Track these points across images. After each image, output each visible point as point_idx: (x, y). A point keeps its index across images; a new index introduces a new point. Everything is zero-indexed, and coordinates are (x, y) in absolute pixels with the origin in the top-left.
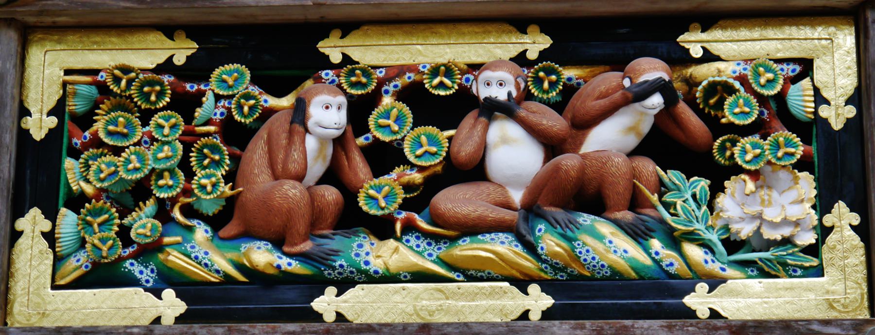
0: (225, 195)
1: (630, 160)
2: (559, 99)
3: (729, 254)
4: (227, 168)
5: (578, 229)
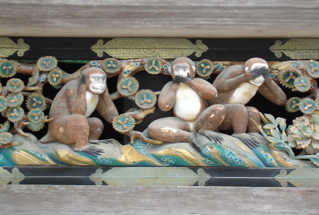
0: (44, 122)
1: (247, 109)
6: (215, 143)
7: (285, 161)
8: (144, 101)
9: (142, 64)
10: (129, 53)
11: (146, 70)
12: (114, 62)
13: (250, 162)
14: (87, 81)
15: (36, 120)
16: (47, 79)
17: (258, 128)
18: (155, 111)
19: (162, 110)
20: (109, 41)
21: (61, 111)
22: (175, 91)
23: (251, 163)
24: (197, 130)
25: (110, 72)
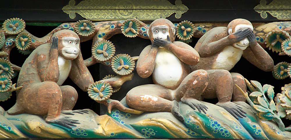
0: (12, 90)
1: (231, 75)
2: (191, 41)
4: (13, 76)
5: (207, 110)
6: (199, 112)
8: (121, 67)
10: (104, 15)
11: (123, 32)
13: (237, 134)
14: (59, 45)
15: (3, 89)
16: (14, 43)
17: (244, 96)
18: (133, 78)
19: (141, 76)
22: (155, 56)
23: (238, 134)
25: (83, 35)
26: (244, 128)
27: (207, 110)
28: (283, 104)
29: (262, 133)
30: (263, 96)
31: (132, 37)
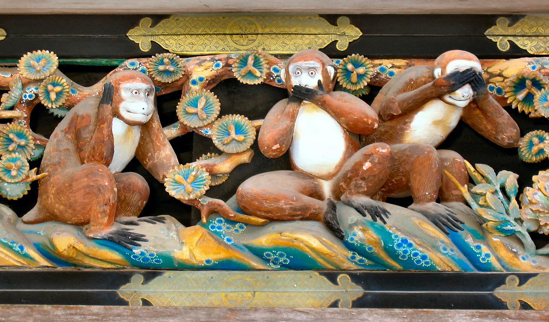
0: (30, 179)
2: (366, 93)
3: (538, 247)
5: (387, 217)
6: (372, 221)
7: (515, 259)
8: (230, 139)
9: (228, 65)
11: (236, 75)
12: (172, 61)
14: (115, 97)
15: (14, 177)
16: (37, 95)
17: (461, 191)
19: (267, 155)
20: (164, 21)
21: (62, 157)
22: (293, 117)
24: (337, 192)
26: (458, 250)
27: (387, 217)
28: (535, 206)
29: (492, 260)
30: (496, 191)
31: (252, 84)
